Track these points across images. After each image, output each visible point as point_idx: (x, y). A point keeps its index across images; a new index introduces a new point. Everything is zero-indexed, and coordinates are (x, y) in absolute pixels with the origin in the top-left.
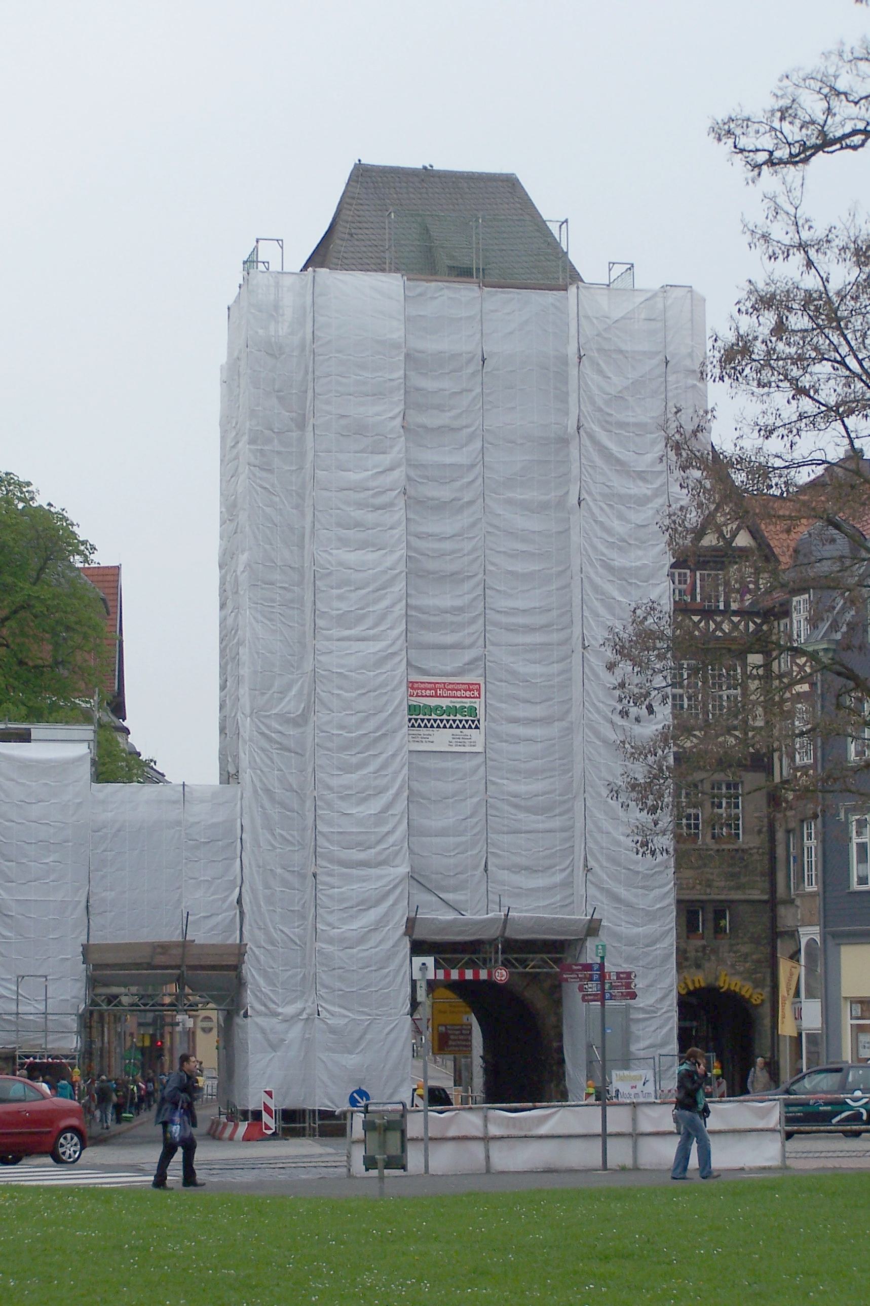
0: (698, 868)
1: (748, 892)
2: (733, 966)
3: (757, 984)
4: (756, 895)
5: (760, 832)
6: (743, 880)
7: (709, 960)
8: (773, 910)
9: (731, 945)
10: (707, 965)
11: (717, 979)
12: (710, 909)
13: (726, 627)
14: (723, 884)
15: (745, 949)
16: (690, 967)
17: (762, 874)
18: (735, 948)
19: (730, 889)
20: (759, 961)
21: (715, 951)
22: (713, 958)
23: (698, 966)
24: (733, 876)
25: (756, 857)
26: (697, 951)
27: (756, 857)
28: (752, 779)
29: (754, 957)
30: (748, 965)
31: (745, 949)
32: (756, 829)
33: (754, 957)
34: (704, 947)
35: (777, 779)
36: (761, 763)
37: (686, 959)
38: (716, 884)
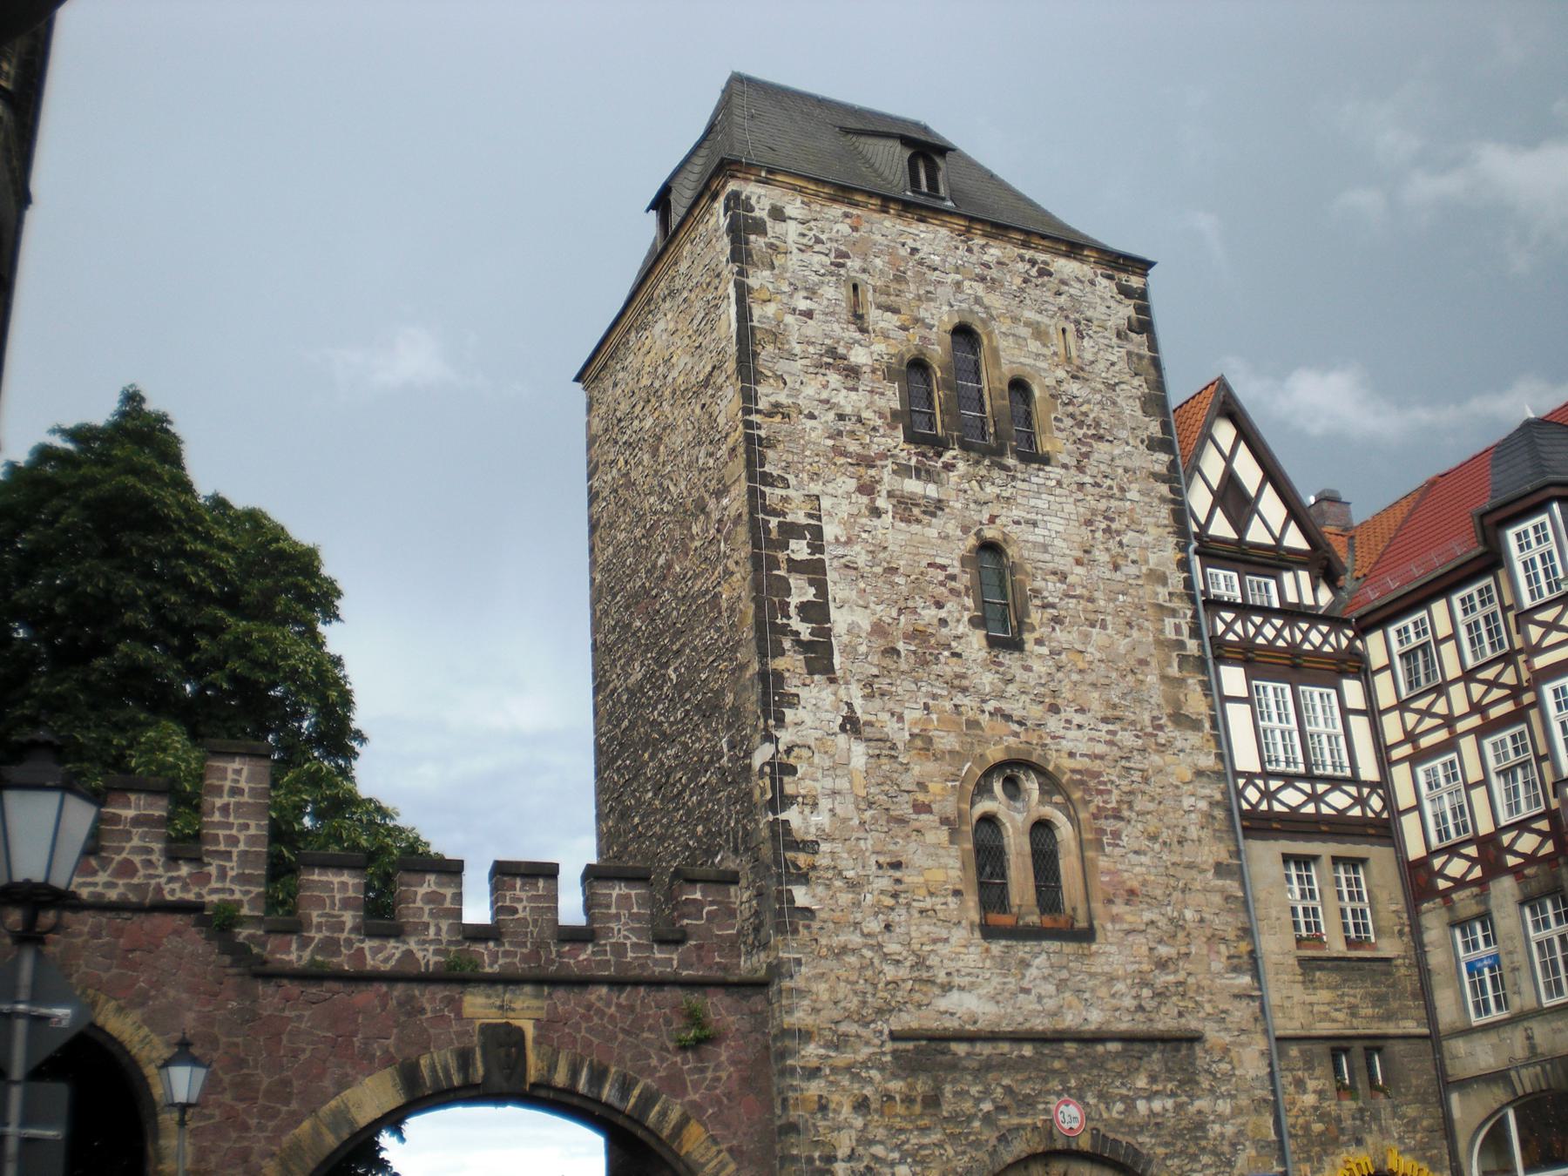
0: (1336, 988)
1: (1401, 1024)
2: (1401, 1139)
4: (1411, 1027)
5: (1401, 933)
6: (1395, 1005)
7: (1371, 1132)
8: (1437, 1049)
9: (1395, 1107)
10: (1370, 1140)
11: (1385, 1161)
12: (1358, 1047)
13: (1315, 637)
14: (1370, 1011)
17: (1414, 996)
20: (1430, 1130)
21: (1375, 1117)
22: (1375, 1127)
23: (1359, 1142)
24: (1379, 1000)
25: (1403, 971)
26: (1354, 1119)
27: (1403, 971)
28: (1379, 856)
30: (1418, 1136)
31: (1411, 1111)
32: (1396, 929)
33: (1425, 1123)
34: (1361, 1110)
35: (1415, 850)
36: (1385, 830)
37: (1342, 1131)
38: (1363, 1012)
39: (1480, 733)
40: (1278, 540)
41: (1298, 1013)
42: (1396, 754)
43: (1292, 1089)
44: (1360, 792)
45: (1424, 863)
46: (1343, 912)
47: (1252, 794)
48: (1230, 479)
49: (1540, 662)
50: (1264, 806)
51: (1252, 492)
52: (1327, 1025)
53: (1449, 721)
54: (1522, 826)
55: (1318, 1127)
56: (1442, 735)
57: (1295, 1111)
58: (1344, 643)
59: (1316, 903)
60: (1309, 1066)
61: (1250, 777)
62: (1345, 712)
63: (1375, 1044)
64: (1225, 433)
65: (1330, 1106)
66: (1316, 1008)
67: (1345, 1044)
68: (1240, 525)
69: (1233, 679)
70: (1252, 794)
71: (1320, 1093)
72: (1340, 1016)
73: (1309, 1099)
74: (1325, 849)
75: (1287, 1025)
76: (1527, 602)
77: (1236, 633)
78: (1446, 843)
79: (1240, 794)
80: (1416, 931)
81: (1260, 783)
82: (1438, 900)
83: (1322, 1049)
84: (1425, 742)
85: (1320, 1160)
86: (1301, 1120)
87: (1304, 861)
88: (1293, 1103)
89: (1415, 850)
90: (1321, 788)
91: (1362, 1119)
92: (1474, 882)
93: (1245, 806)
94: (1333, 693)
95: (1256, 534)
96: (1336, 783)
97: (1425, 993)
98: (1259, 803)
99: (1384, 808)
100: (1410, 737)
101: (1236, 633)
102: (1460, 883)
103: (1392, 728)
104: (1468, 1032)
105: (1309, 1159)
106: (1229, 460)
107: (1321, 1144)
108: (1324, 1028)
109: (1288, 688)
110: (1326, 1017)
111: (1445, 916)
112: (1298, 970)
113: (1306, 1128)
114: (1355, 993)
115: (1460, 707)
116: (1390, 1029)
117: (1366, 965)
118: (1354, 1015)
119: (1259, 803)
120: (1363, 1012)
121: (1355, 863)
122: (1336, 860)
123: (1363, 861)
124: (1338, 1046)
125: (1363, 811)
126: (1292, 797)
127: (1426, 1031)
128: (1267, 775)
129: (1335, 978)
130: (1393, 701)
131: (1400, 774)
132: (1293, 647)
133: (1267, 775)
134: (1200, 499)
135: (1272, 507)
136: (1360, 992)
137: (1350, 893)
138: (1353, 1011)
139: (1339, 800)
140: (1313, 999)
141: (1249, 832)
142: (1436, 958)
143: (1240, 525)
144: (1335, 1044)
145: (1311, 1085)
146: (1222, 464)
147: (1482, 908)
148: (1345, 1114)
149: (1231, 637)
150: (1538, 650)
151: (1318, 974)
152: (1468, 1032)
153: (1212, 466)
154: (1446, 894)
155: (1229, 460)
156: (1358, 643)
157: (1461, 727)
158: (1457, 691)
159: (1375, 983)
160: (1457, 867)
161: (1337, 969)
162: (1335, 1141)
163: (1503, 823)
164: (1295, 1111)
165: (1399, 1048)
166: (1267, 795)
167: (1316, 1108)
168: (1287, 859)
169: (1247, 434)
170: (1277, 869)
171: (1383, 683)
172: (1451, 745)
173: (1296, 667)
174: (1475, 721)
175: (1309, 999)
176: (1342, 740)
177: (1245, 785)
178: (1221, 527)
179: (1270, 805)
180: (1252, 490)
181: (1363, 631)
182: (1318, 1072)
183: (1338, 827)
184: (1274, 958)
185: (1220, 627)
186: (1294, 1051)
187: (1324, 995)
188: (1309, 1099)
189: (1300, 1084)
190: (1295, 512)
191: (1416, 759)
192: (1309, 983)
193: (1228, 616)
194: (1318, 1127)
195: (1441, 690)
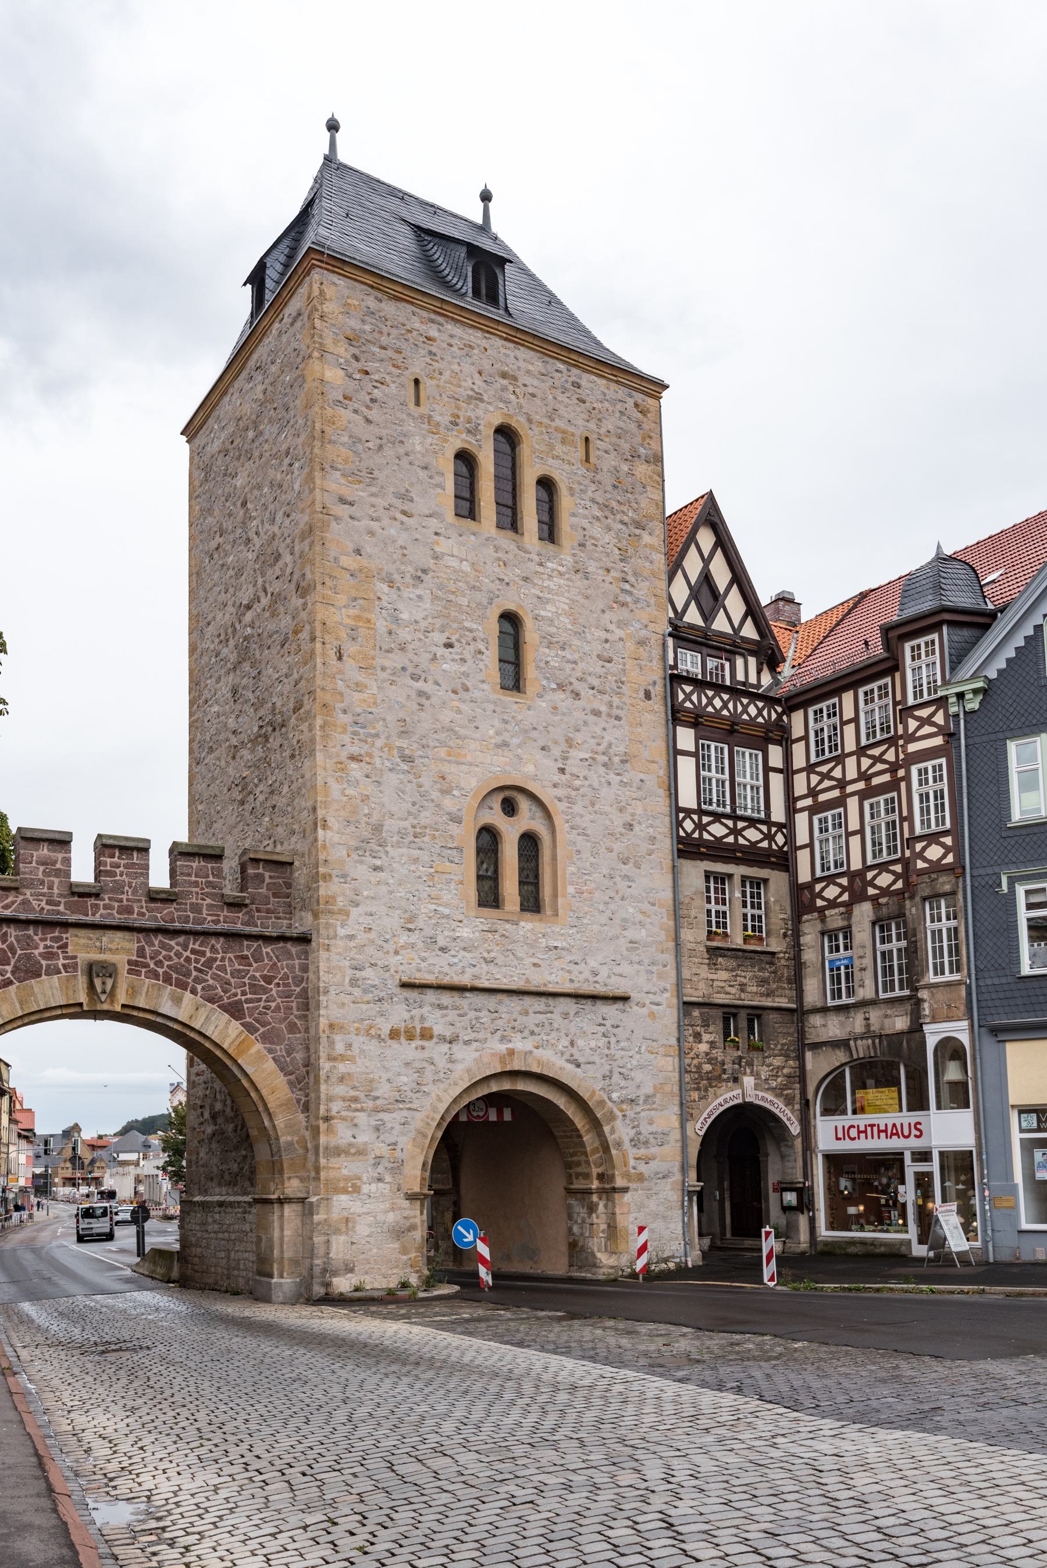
0: (732, 970)
3: (789, 1101)
4: (783, 1002)
5: (785, 935)
12: (743, 1014)
13: (753, 711)
14: (754, 989)
15: (777, 1062)
16: (727, 1080)
17: (789, 982)
18: (767, 1061)
19: (762, 995)
20: (789, 1076)
21: (750, 1064)
22: (748, 1071)
24: (763, 982)
25: (783, 962)
27: (783, 962)
29: (785, 1071)
33: (785, 1071)
34: (740, 1058)
35: (804, 876)
37: (724, 1071)
38: (749, 989)
39: (863, 795)
40: (737, 631)
41: (702, 985)
42: (800, 804)
43: (691, 1039)
44: (769, 830)
45: (809, 886)
46: (745, 916)
47: (688, 825)
48: (706, 577)
49: (912, 748)
50: (696, 835)
51: (722, 590)
52: (722, 996)
53: (842, 784)
54: (883, 867)
55: (707, 1067)
56: (836, 793)
57: (692, 1055)
58: (774, 716)
59: (726, 908)
60: (706, 1025)
61: (688, 812)
62: (767, 769)
63: (756, 1013)
64: (706, 539)
65: (718, 1054)
66: (716, 984)
67: (734, 1011)
68: (708, 616)
69: (686, 738)
70: (688, 825)
71: (712, 1044)
72: (733, 990)
73: (704, 1047)
74: (738, 871)
75: (694, 995)
76: (911, 701)
77: (692, 702)
78: (826, 873)
79: (679, 824)
80: (797, 934)
81: (695, 817)
82: (816, 914)
83: (718, 1013)
84: (822, 798)
85: (706, 1090)
86: (695, 1062)
87: (722, 879)
88: (691, 1049)
89: (804, 876)
90: (741, 825)
91: (739, 1064)
92: (843, 904)
93: (682, 833)
94: (760, 754)
95: (720, 624)
96: (752, 822)
97: (797, 980)
98: (693, 831)
99: (785, 843)
100: (813, 793)
101: (692, 702)
102: (832, 904)
103: (800, 785)
104: (824, 1010)
105: (698, 1089)
106: (707, 561)
107: (708, 1079)
108: (720, 999)
109: (726, 747)
110: (722, 990)
111: (819, 927)
112: (706, 956)
113: (699, 1067)
114: (747, 976)
115: (852, 773)
116: (768, 1002)
117: (756, 956)
118: (742, 991)
119: (693, 831)
120: (749, 989)
121: (759, 883)
122: (744, 879)
123: (766, 881)
124: (729, 1013)
125: (770, 844)
126: (718, 830)
127: (794, 1006)
128: (701, 812)
129: (732, 963)
130: (804, 765)
131: (801, 820)
132: (734, 714)
133: (701, 812)
134: (680, 592)
135: (734, 603)
136: (749, 974)
137: (752, 903)
138: (743, 987)
139: (752, 834)
140: (714, 977)
141: (682, 854)
142: (809, 956)
143: (708, 616)
144: (726, 1010)
145: (706, 1037)
146: (700, 565)
147: (845, 923)
148: (728, 1059)
149: (688, 704)
150: (912, 738)
151: (720, 959)
152: (824, 1010)
153: (693, 565)
154: (821, 910)
155: (707, 561)
156: (785, 718)
157: (850, 789)
158: (851, 763)
159: (761, 970)
160: (831, 892)
161: (737, 958)
162: (719, 1078)
163: (869, 863)
164: (692, 1055)
165: (773, 1016)
166: (701, 827)
167: (707, 1054)
168: (708, 875)
169: (724, 543)
170: (700, 883)
171: (798, 749)
172: (840, 802)
173: (732, 732)
174: (861, 785)
175: (711, 976)
176: (761, 790)
177: (684, 819)
178: (693, 616)
179: (701, 834)
180: (722, 587)
181: (790, 709)
182: (711, 1029)
183: (751, 856)
184: (690, 946)
185: (681, 696)
186: (696, 1013)
187: (724, 975)
188: (704, 1047)
189: (698, 1037)
190: (753, 609)
191: (813, 810)
192: (713, 965)
193: (688, 689)
194: (707, 1067)
195: (840, 760)
